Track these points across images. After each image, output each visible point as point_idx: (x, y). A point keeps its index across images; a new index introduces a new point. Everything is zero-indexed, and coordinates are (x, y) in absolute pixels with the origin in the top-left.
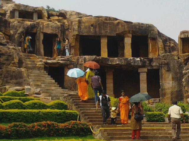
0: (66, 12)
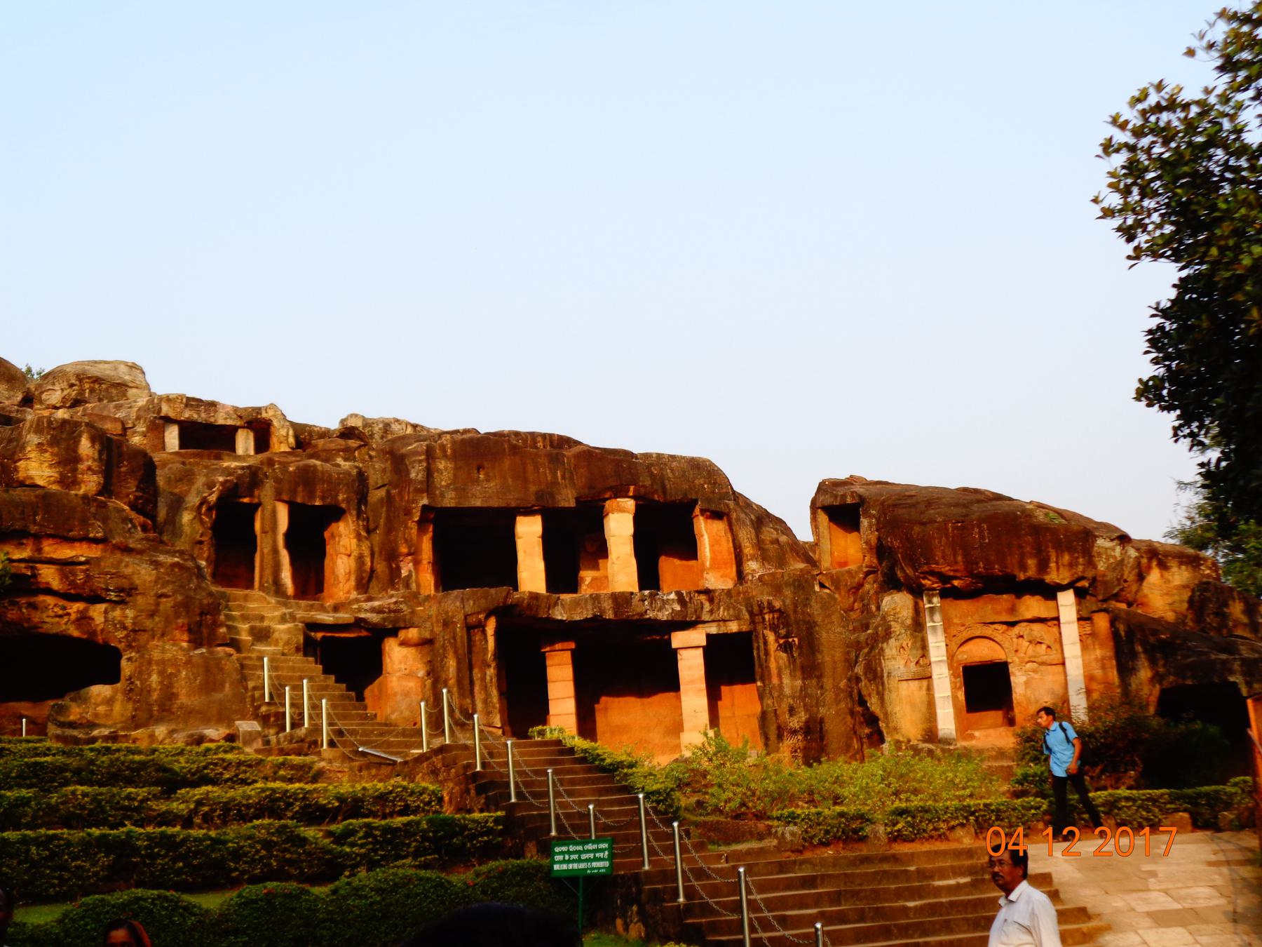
0: (368, 423)
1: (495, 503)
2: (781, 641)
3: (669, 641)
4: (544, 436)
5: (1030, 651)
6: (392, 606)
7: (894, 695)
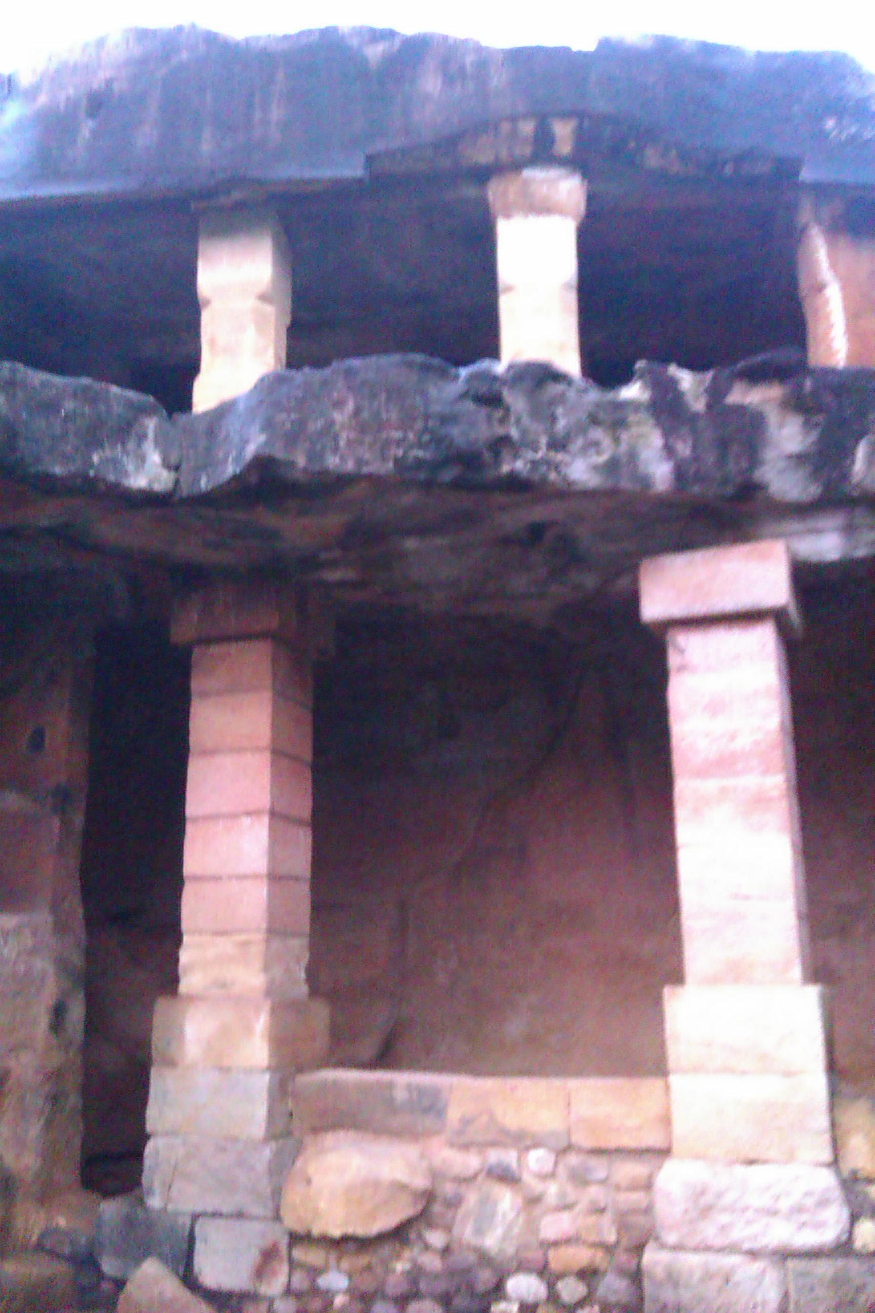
3: (633, 600)
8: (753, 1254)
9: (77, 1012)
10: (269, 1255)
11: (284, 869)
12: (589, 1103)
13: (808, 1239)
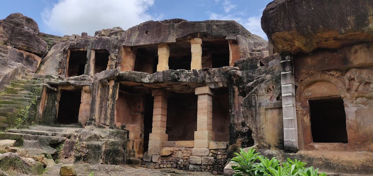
1: (148, 43)
2: (241, 91)
4: (173, 20)
5: (361, 88)
6: (82, 78)
7: (262, 117)
8: (200, 156)
9: (143, 136)
10: (159, 158)
11: (163, 120)
12: (188, 143)
13: (205, 155)
